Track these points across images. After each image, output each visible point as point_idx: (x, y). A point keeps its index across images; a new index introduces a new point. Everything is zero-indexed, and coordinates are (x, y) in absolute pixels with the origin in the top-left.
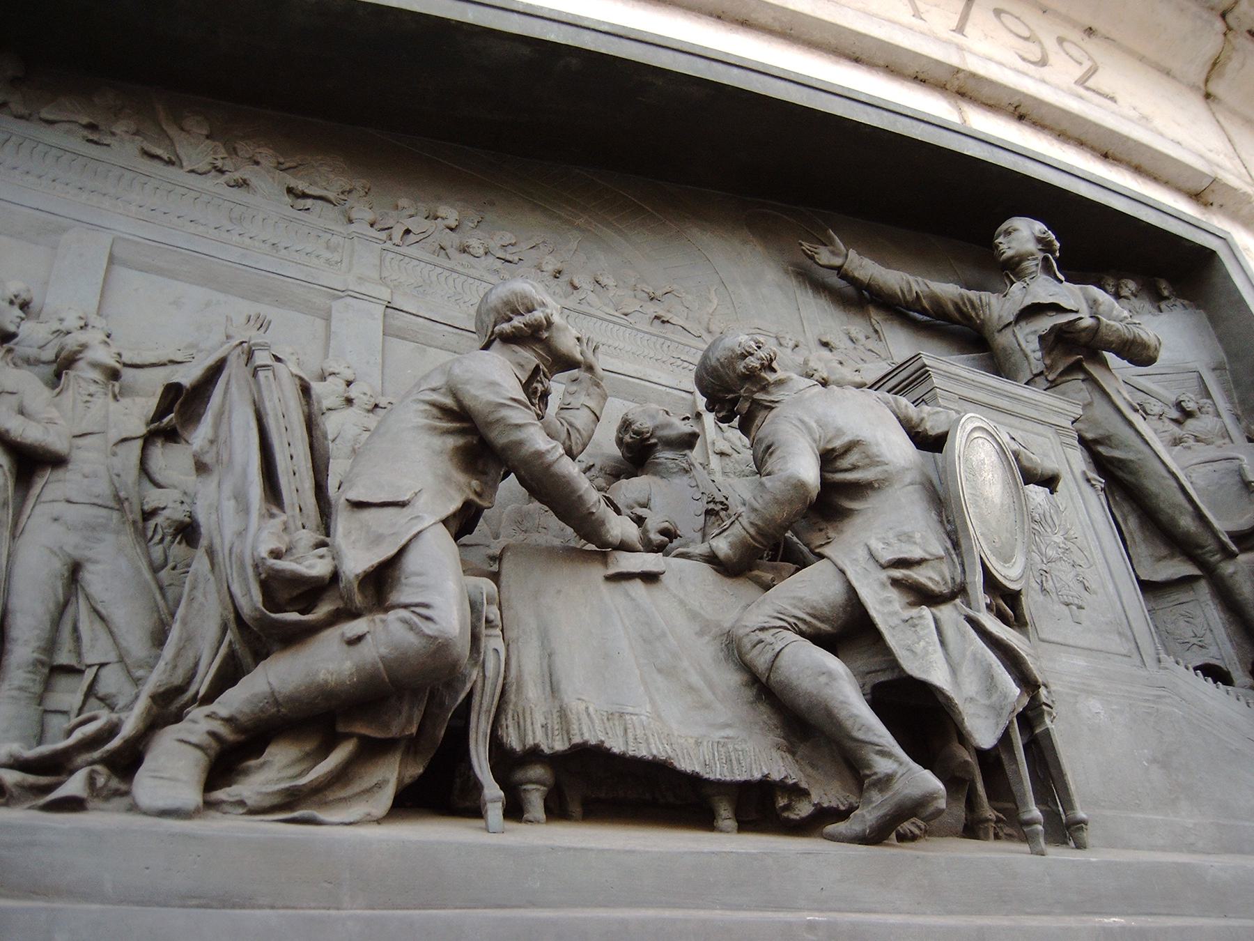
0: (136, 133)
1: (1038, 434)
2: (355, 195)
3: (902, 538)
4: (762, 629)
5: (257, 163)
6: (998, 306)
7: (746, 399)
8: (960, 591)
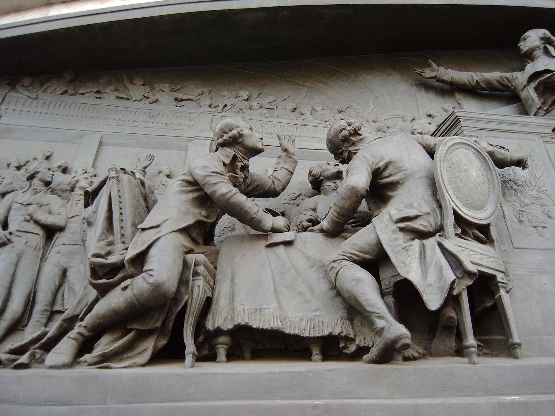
0: (116, 90)
1: (528, 140)
2: (204, 95)
3: (408, 206)
4: (334, 261)
5: (163, 91)
6: (520, 78)
8: (440, 230)
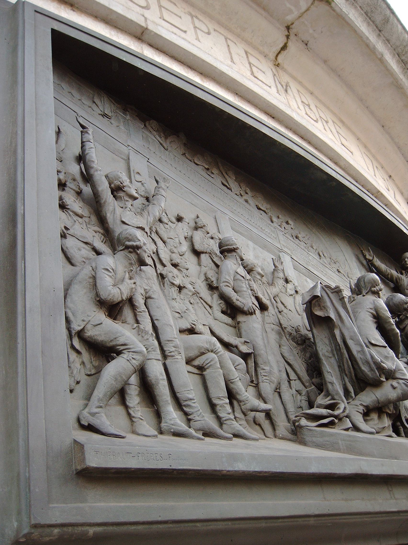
7: (404, 315)
